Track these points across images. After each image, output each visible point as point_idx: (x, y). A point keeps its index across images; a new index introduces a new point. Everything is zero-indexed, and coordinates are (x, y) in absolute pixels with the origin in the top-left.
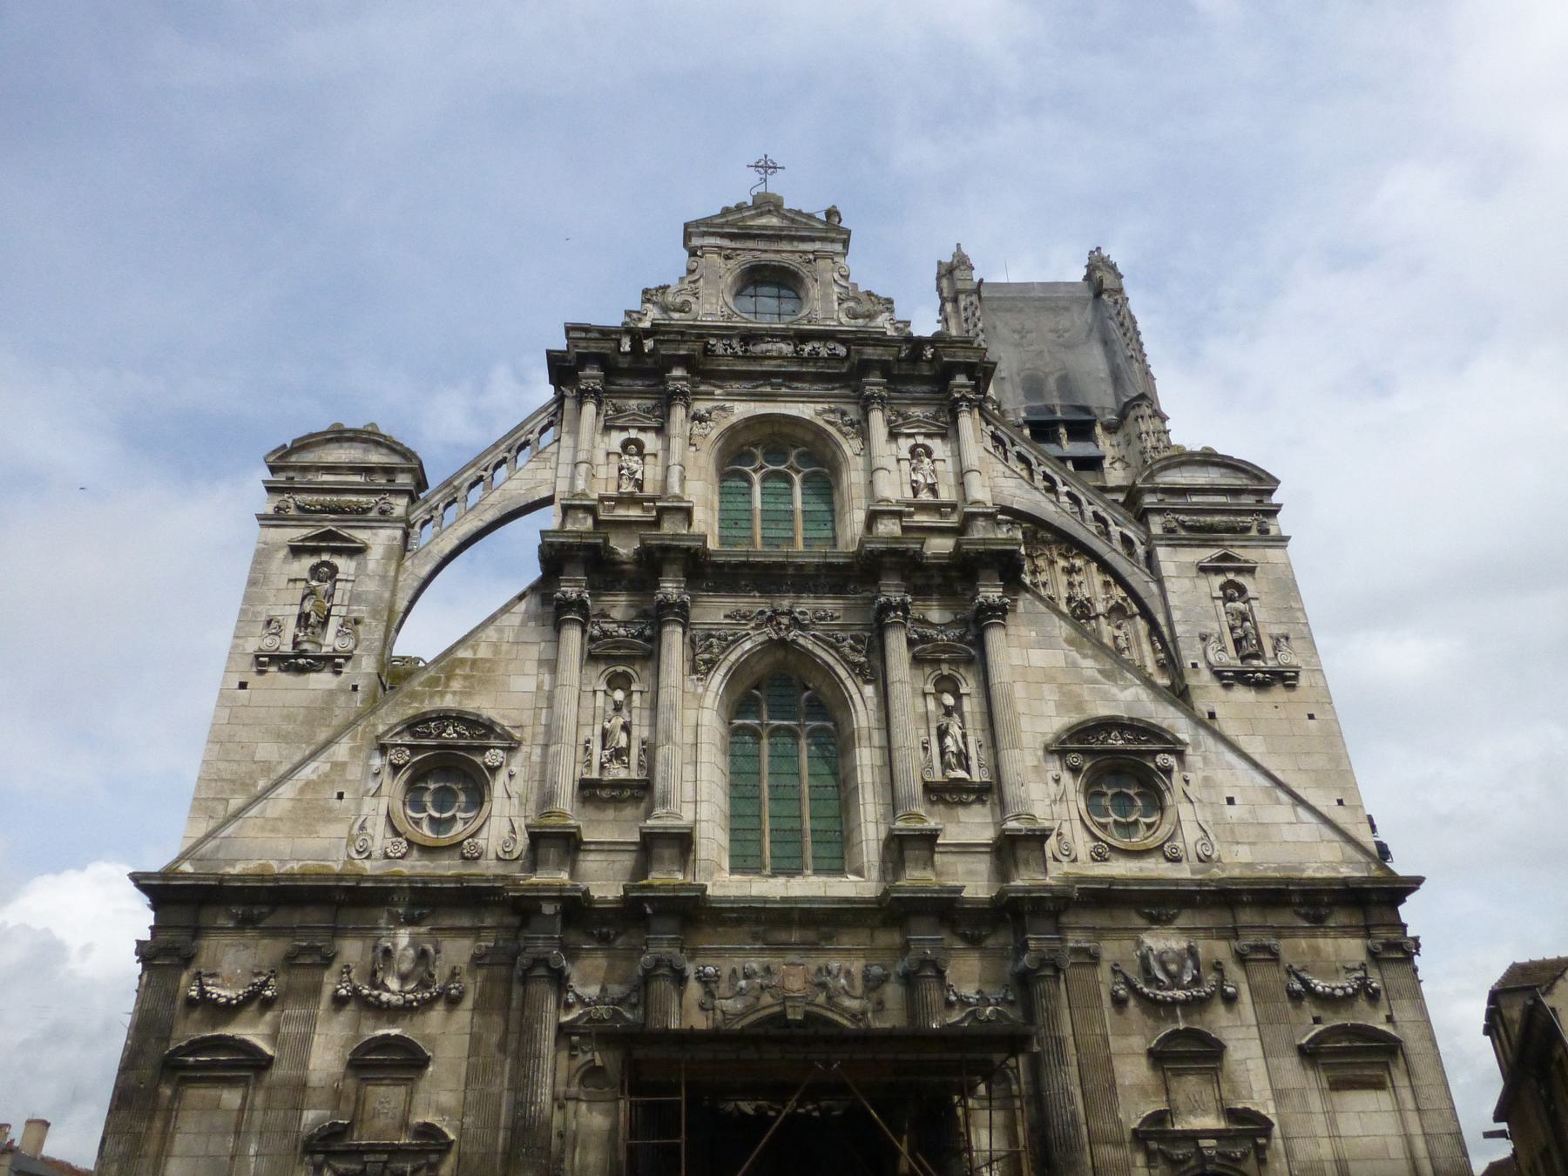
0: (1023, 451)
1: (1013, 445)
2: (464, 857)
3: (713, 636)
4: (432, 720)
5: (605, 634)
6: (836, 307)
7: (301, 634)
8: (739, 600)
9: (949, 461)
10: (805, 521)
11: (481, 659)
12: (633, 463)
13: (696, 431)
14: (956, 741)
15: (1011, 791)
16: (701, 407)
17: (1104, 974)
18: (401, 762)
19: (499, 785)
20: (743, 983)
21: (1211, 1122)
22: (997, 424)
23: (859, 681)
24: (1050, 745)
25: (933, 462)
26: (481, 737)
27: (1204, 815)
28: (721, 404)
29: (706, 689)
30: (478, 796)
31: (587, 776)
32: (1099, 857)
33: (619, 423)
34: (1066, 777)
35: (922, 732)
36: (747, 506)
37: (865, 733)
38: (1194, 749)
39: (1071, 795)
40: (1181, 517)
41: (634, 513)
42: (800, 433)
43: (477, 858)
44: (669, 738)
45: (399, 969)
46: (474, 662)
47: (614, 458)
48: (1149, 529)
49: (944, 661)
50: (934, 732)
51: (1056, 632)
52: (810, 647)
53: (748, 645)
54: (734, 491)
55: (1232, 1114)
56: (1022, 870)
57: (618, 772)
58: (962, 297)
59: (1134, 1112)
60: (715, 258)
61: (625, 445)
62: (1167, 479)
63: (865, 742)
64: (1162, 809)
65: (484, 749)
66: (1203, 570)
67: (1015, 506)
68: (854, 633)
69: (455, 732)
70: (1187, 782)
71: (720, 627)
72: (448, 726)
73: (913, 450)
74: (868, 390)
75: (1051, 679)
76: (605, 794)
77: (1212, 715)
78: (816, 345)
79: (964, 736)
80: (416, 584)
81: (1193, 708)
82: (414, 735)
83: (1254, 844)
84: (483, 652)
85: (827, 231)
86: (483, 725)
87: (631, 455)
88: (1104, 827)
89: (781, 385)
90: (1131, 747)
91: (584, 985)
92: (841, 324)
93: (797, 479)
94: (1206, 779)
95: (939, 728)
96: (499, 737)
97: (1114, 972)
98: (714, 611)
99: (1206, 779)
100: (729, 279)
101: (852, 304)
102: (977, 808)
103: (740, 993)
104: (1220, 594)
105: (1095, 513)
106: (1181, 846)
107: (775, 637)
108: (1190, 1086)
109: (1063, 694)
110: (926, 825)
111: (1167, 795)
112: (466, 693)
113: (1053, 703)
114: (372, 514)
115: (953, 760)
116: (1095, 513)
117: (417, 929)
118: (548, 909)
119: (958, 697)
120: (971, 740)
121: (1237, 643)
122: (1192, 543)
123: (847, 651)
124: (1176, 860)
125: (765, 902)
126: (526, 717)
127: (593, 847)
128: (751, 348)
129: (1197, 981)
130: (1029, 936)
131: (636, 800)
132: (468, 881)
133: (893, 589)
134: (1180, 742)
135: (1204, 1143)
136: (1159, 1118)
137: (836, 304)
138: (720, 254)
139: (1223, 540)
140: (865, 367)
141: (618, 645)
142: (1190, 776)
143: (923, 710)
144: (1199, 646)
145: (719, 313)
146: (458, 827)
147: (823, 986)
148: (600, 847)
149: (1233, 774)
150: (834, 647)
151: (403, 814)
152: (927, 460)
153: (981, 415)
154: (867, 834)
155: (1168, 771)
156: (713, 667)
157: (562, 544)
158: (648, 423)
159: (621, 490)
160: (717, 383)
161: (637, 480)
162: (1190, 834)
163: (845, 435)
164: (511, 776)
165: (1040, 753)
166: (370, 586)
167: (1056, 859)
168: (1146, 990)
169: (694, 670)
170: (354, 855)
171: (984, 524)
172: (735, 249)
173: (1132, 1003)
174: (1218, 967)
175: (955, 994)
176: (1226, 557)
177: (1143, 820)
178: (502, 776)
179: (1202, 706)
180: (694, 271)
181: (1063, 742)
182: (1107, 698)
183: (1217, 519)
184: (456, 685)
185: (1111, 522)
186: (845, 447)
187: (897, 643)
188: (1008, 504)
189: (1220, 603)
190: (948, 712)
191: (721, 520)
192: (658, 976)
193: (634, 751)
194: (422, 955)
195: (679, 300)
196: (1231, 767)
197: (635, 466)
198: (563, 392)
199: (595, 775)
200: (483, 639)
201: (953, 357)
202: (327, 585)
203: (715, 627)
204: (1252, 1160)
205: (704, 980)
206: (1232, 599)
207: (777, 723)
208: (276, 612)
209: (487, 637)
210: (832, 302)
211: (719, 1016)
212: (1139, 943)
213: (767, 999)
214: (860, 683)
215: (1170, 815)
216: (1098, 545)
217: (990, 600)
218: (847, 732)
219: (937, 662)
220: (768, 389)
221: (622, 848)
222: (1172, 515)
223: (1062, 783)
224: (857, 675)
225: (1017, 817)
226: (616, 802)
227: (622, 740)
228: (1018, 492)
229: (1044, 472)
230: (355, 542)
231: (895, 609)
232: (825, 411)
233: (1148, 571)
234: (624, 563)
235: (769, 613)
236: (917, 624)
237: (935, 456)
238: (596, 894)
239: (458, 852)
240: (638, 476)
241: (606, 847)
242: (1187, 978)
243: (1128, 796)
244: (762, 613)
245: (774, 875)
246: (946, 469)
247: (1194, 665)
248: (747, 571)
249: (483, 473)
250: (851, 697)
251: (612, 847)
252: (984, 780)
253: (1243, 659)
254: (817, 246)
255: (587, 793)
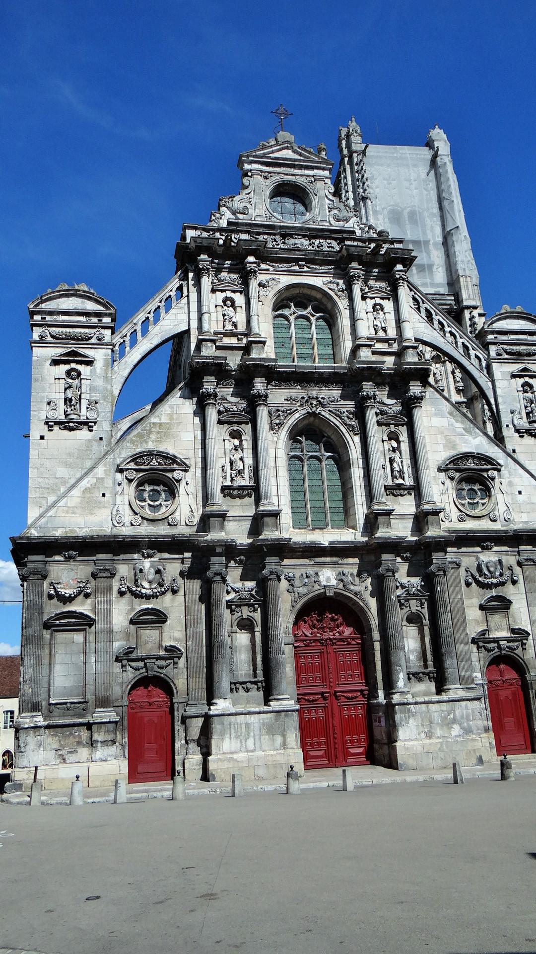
0: (428, 307)
1: (423, 303)
2: (169, 524)
3: (278, 410)
4: (145, 456)
5: (227, 410)
6: (328, 213)
7: (69, 410)
8: (291, 391)
9: (393, 313)
10: (318, 344)
11: (164, 423)
12: (230, 311)
13: (261, 293)
14: (399, 465)
15: (425, 490)
16: (262, 278)
17: (462, 571)
18: (132, 478)
19: (182, 488)
20: (306, 580)
21: (505, 634)
22: (416, 291)
23: (351, 433)
24: (441, 467)
25: (384, 313)
26: (170, 464)
27: (508, 499)
28: (274, 276)
29: (278, 439)
30: (172, 493)
31: (225, 484)
32: (461, 520)
33: (220, 287)
34: (448, 481)
35: (382, 460)
36: (288, 335)
37: (355, 461)
38: (505, 468)
39: (450, 491)
40: (505, 347)
41: (233, 341)
42: (314, 293)
43: (176, 525)
44: (265, 466)
45: (148, 578)
46: (161, 424)
47: (219, 308)
48: (489, 353)
49: (392, 424)
50: (388, 460)
51: (444, 409)
52: (328, 417)
53: (297, 415)
54: (280, 326)
55: (513, 631)
56: (430, 527)
57: (239, 482)
58: (355, 155)
59: (473, 630)
60: (260, 179)
61: (225, 301)
62: (499, 325)
63: (356, 465)
64: (490, 496)
65: (173, 470)
66: (514, 376)
67: (424, 339)
68: (348, 409)
69: (157, 462)
70: (501, 484)
71: (282, 405)
72: (153, 459)
73: (374, 307)
74: (352, 273)
75: (442, 433)
76: (235, 493)
77: (514, 451)
78: (321, 241)
79: (402, 462)
80: (123, 380)
81: (505, 447)
82: (136, 464)
83: (529, 512)
84: (164, 419)
85: (320, 163)
86: (171, 459)
87: (228, 307)
88: (463, 505)
89: (304, 265)
90: (476, 467)
91: (234, 583)
92: (331, 225)
93: (313, 319)
94: (510, 482)
95: (390, 458)
96: (178, 464)
97: (467, 571)
98: (278, 396)
99: (510, 482)
100: (268, 193)
101: (336, 212)
102: (408, 497)
103: (306, 584)
104: (521, 389)
105: (463, 343)
106: (497, 514)
107: (311, 411)
108: (497, 619)
109: (447, 440)
110: (388, 508)
111: (492, 489)
112: (159, 441)
113: (442, 445)
114: (94, 340)
115: (398, 475)
116: (463, 343)
117: (152, 559)
118: (219, 550)
119: (399, 442)
120: (405, 464)
121: (528, 414)
122: (510, 361)
123: (346, 418)
124: (494, 521)
125: (316, 544)
126: (191, 454)
127: (231, 518)
128: (287, 241)
129: (501, 575)
130: (433, 557)
131: (249, 495)
132: (177, 537)
133: (369, 387)
134: (499, 464)
135: (501, 643)
136: (483, 633)
137: (327, 211)
138: (261, 175)
139: (524, 360)
140: (351, 258)
141: (234, 414)
142: (503, 481)
143: (382, 449)
144: (511, 415)
145: (264, 215)
146: (163, 509)
147: (342, 580)
148: (234, 518)
149: (522, 480)
150: (339, 415)
151: (136, 504)
152: (381, 313)
153: (408, 286)
154: (358, 511)
155: (493, 479)
156: (281, 426)
157: (204, 363)
158: (236, 288)
159: (226, 328)
160: (271, 264)
161: (233, 322)
162: (502, 508)
163: (339, 297)
164: (187, 484)
165: (436, 470)
166: (100, 382)
167: (443, 521)
168: (480, 579)
169: (272, 429)
170: (116, 524)
171: (412, 352)
172: (269, 173)
173: (474, 584)
174: (510, 568)
175: (399, 582)
176: (525, 370)
177: (480, 501)
178: (183, 483)
179: (509, 447)
180: (248, 187)
181: (447, 465)
182: (466, 442)
183: (522, 348)
184: (153, 437)
185: (470, 348)
186: (339, 304)
187: (371, 417)
188: (421, 338)
189: (521, 393)
190: (394, 450)
191: (275, 343)
192: (271, 579)
193: (247, 471)
194: (158, 572)
195: (242, 206)
196: (521, 476)
197: (232, 314)
198: (187, 267)
199: (229, 483)
200: (163, 412)
201: (396, 254)
202: (77, 381)
203: (280, 405)
204: (520, 648)
205: (289, 579)
206: (525, 391)
207: (310, 454)
208: (53, 397)
209: (166, 411)
210: (325, 210)
211: (297, 595)
212: (478, 558)
213: (317, 587)
214: (352, 435)
215: (493, 499)
216: (464, 361)
217: (416, 394)
218: (346, 459)
219: (388, 425)
220: (297, 268)
221: (245, 518)
222: (501, 346)
223: (446, 485)
224: (350, 431)
225: (428, 503)
226: (241, 497)
227: (240, 465)
228: (426, 331)
229: (439, 319)
230: (88, 357)
231: (370, 398)
232: (328, 282)
233: (487, 376)
234: (233, 371)
235: (306, 398)
236: (378, 404)
237: (385, 311)
238: (238, 542)
239: (166, 521)
240: (234, 320)
241: (238, 518)
242: (498, 574)
243: (474, 490)
244: (303, 398)
245: (314, 529)
246: (391, 317)
247: (507, 426)
248: (294, 376)
249: (149, 315)
250: (348, 442)
251: (241, 518)
252: (411, 484)
253: (530, 423)
254: (316, 172)
255: (226, 492)
